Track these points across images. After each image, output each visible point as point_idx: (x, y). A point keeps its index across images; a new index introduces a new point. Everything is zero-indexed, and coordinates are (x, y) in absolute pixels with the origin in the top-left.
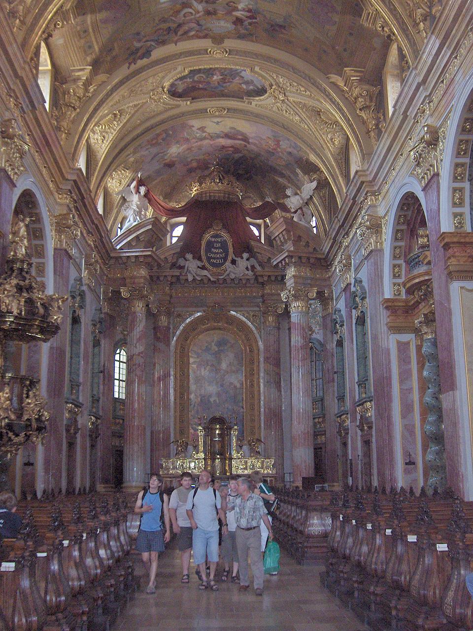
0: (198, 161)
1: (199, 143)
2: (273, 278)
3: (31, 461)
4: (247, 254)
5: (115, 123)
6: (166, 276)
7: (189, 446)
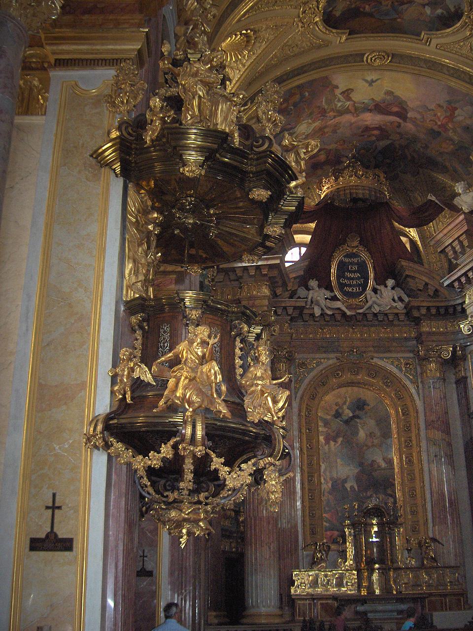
0: (328, 152)
1: (338, 119)
2: (433, 311)
3: (149, 567)
4: (393, 280)
5: (246, 52)
6: (285, 308)
7: (330, 552)
